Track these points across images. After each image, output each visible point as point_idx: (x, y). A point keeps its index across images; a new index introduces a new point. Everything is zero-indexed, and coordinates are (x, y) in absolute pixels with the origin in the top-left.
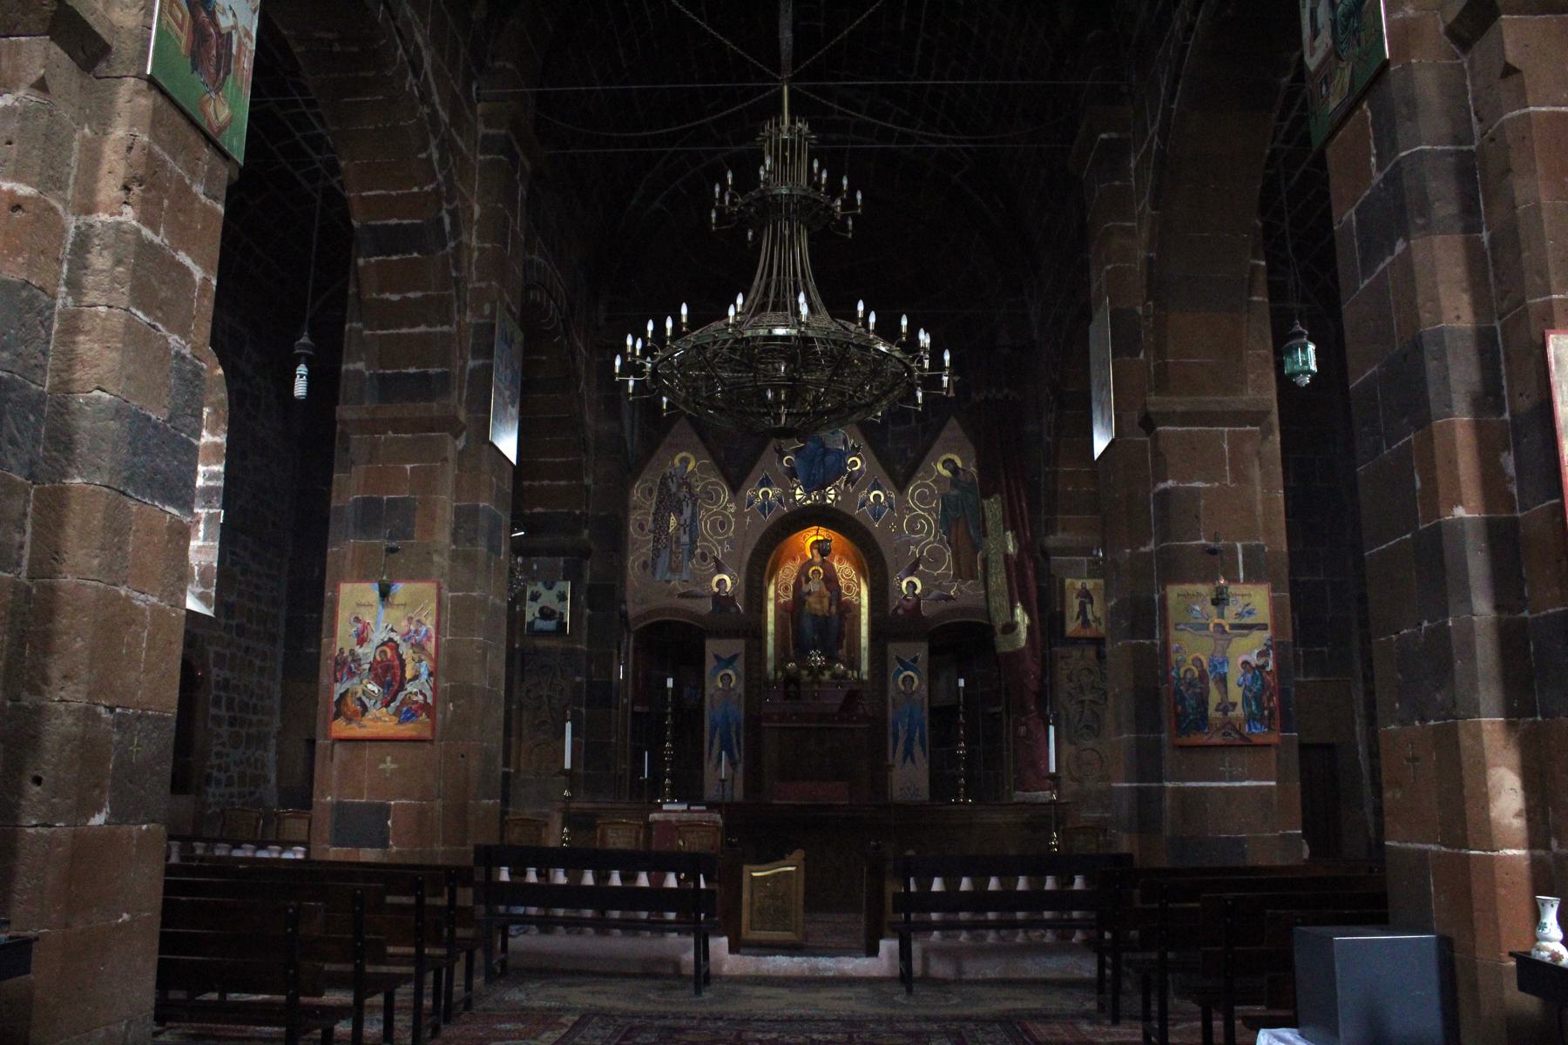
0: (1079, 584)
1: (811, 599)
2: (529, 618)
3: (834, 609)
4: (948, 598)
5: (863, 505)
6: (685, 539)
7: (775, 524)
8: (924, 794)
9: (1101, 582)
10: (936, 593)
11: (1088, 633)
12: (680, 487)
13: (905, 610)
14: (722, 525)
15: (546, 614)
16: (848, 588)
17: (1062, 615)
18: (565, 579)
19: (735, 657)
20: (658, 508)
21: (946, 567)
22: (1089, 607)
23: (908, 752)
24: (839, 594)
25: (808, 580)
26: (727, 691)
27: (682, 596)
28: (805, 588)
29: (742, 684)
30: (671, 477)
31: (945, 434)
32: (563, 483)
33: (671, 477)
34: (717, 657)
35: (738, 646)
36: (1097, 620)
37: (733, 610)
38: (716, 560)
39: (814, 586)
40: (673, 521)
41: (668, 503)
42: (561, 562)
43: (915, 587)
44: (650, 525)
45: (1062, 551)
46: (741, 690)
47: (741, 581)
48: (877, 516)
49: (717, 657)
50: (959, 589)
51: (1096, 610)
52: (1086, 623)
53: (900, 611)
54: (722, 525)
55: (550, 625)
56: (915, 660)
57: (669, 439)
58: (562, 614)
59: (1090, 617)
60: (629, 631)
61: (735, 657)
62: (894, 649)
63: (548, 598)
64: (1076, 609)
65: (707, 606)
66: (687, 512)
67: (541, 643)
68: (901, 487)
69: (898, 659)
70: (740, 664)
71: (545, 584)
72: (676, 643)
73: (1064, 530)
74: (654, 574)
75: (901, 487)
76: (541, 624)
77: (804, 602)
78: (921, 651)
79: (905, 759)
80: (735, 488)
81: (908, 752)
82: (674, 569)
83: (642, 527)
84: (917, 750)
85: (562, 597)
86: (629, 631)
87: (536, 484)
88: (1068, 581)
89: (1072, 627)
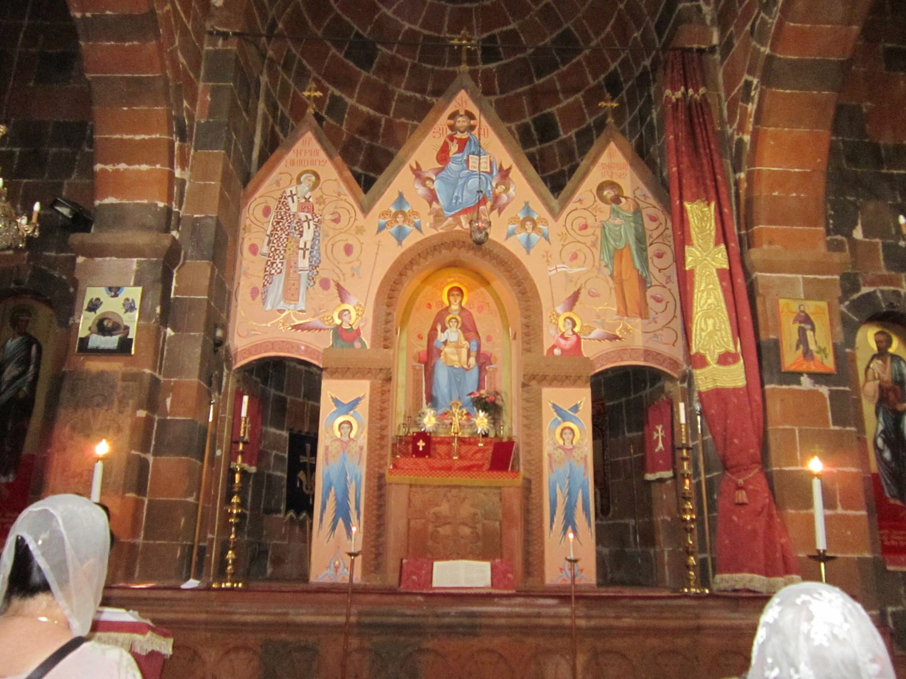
0: (795, 306)
1: (447, 350)
2: (82, 333)
3: (472, 361)
4: (616, 337)
5: (510, 235)
6: (304, 263)
7: (411, 249)
8: (588, 575)
9: (824, 304)
10: (597, 332)
11: (813, 368)
12: (302, 208)
13: (563, 350)
14: (348, 250)
15: (102, 328)
16: (489, 339)
17: (777, 344)
18: (136, 284)
19: (356, 402)
20: (275, 229)
21: (609, 306)
22: (809, 334)
23: (569, 521)
24: (479, 346)
25: (444, 329)
26: (345, 444)
27: (296, 327)
28: (441, 337)
29: (365, 434)
30: (292, 196)
31: (604, 159)
32: (145, 167)
33: (292, 196)
34: (336, 402)
35: (362, 388)
36: (822, 351)
37: (357, 345)
38: (339, 288)
39: (453, 334)
40: (292, 246)
41: (284, 225)
42: (134, 263)
43: (574, 325)
44: (265, 249)
45: (771, 268)
46: (363, 441)
47: (369, 314)
48: (528, 246)
49: (336, 402)
50: (625, 328)
51: (821, 339)
52: (807, 354)
53: (557, 352)
54: (348, 250)
55: (112, 341)
56: (575, 408)
57: (291, 156)
58: (127, 328)
59: (812, 347)
60: (229, 368)
61: (356, 402)
62: (550, 395)
63: (111, 305)
64: (795, 337)
65: (325, 341)
66: (308, 235)
67: (95, 365)
68: (555, 215)
69: (554, 406)
70: (363, 409)
71: (110, 289)
72: (285, 388)
73: (771, 243)
74: (264, 301)
75: (555, 215)
76: (98, 341)
77: (439, 352)
78: (583, 397)
79: (565, 530)
80: (365, 210)
81: (569, 521)
82: (290, 294)
83: (254, 249)
84: (579, 517)
85: (129, 307)
86: (229, 368)
87: (109, 168)
88: (782, 302)
89: (791, 358)
